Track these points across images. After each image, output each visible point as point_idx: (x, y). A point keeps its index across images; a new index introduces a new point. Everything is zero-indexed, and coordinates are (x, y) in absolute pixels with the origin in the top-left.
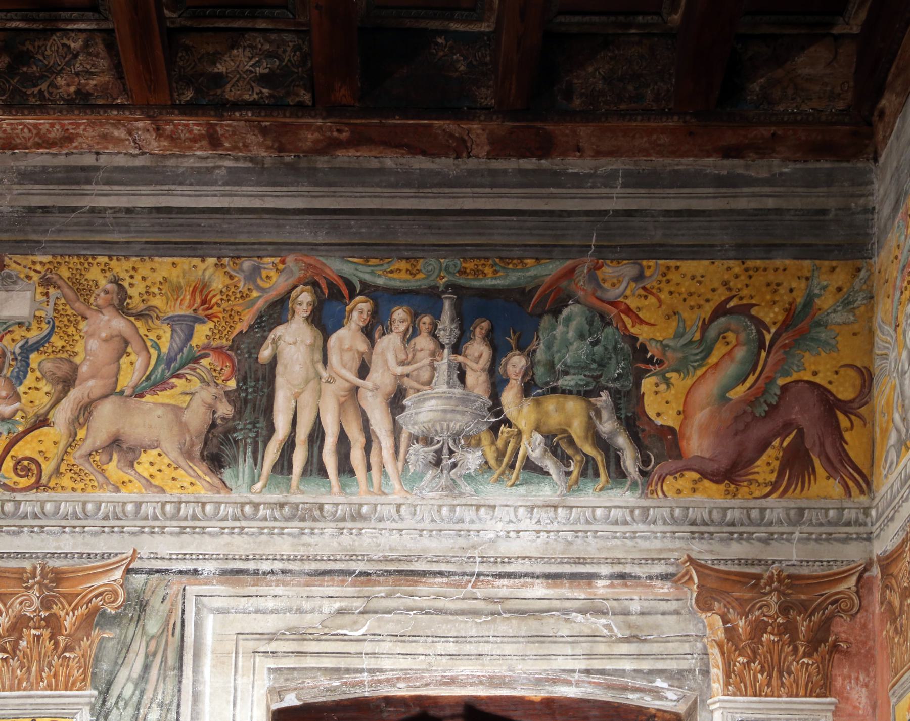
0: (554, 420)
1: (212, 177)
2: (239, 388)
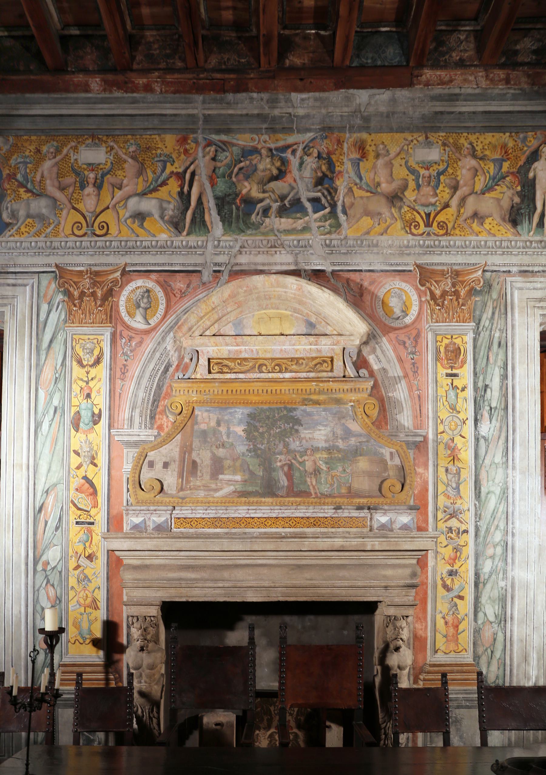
2: (522, 190)
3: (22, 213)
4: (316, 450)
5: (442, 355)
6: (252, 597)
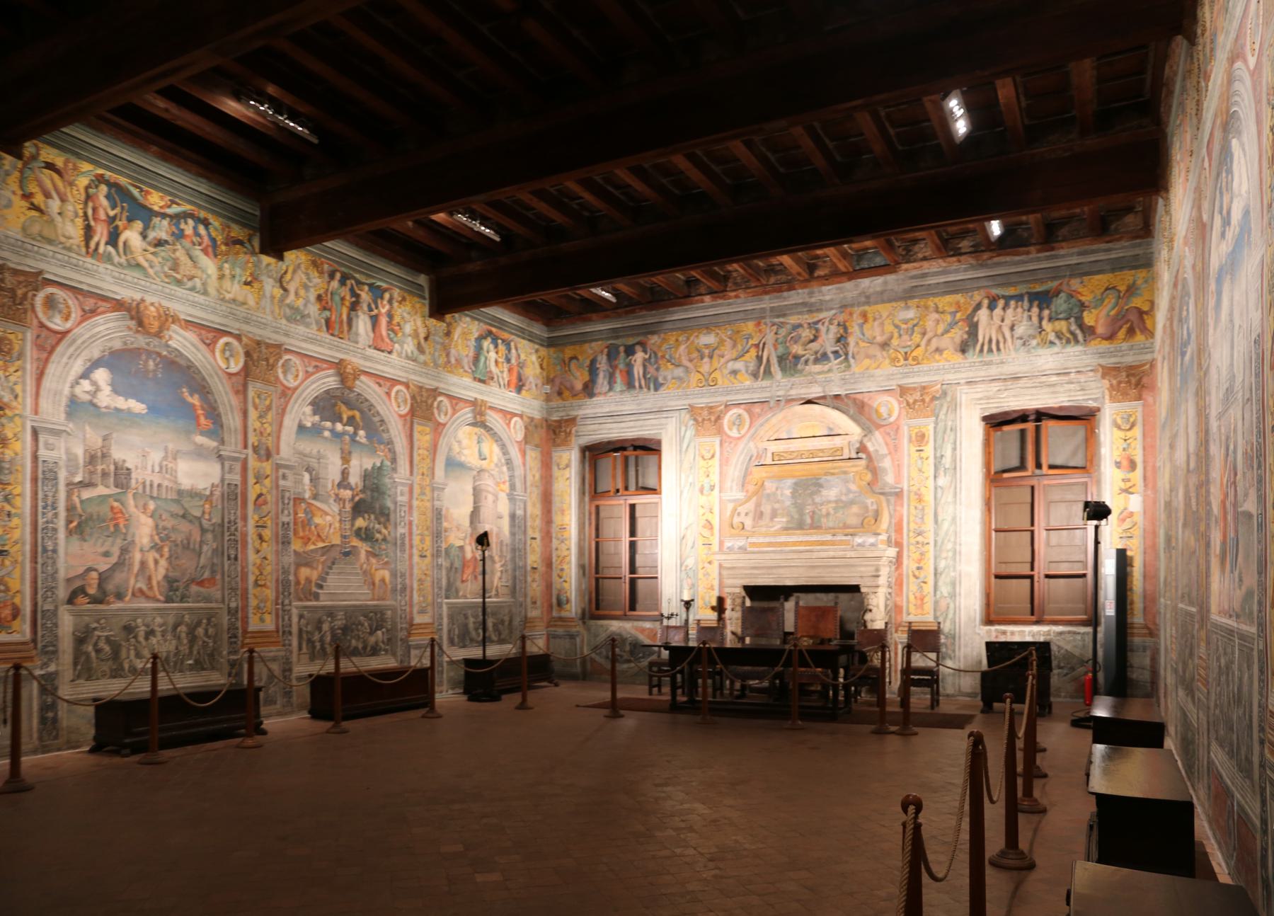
3: (669, 377)
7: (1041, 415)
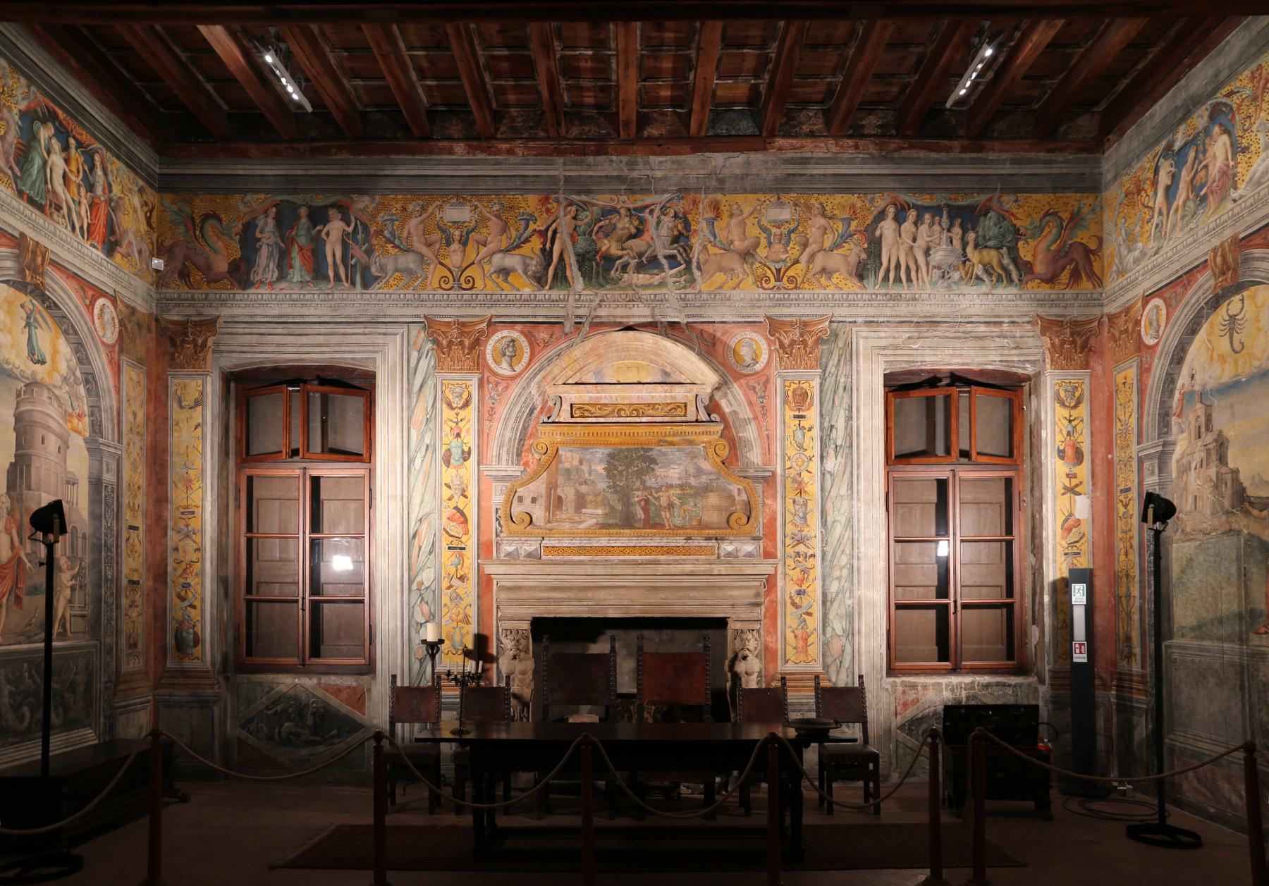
0: (986, 259)
1: (852, 160)
3: (390, 267)
4: (670, 486)
5: (790, 398)
6: (613, 613)
7: (957, 379)
